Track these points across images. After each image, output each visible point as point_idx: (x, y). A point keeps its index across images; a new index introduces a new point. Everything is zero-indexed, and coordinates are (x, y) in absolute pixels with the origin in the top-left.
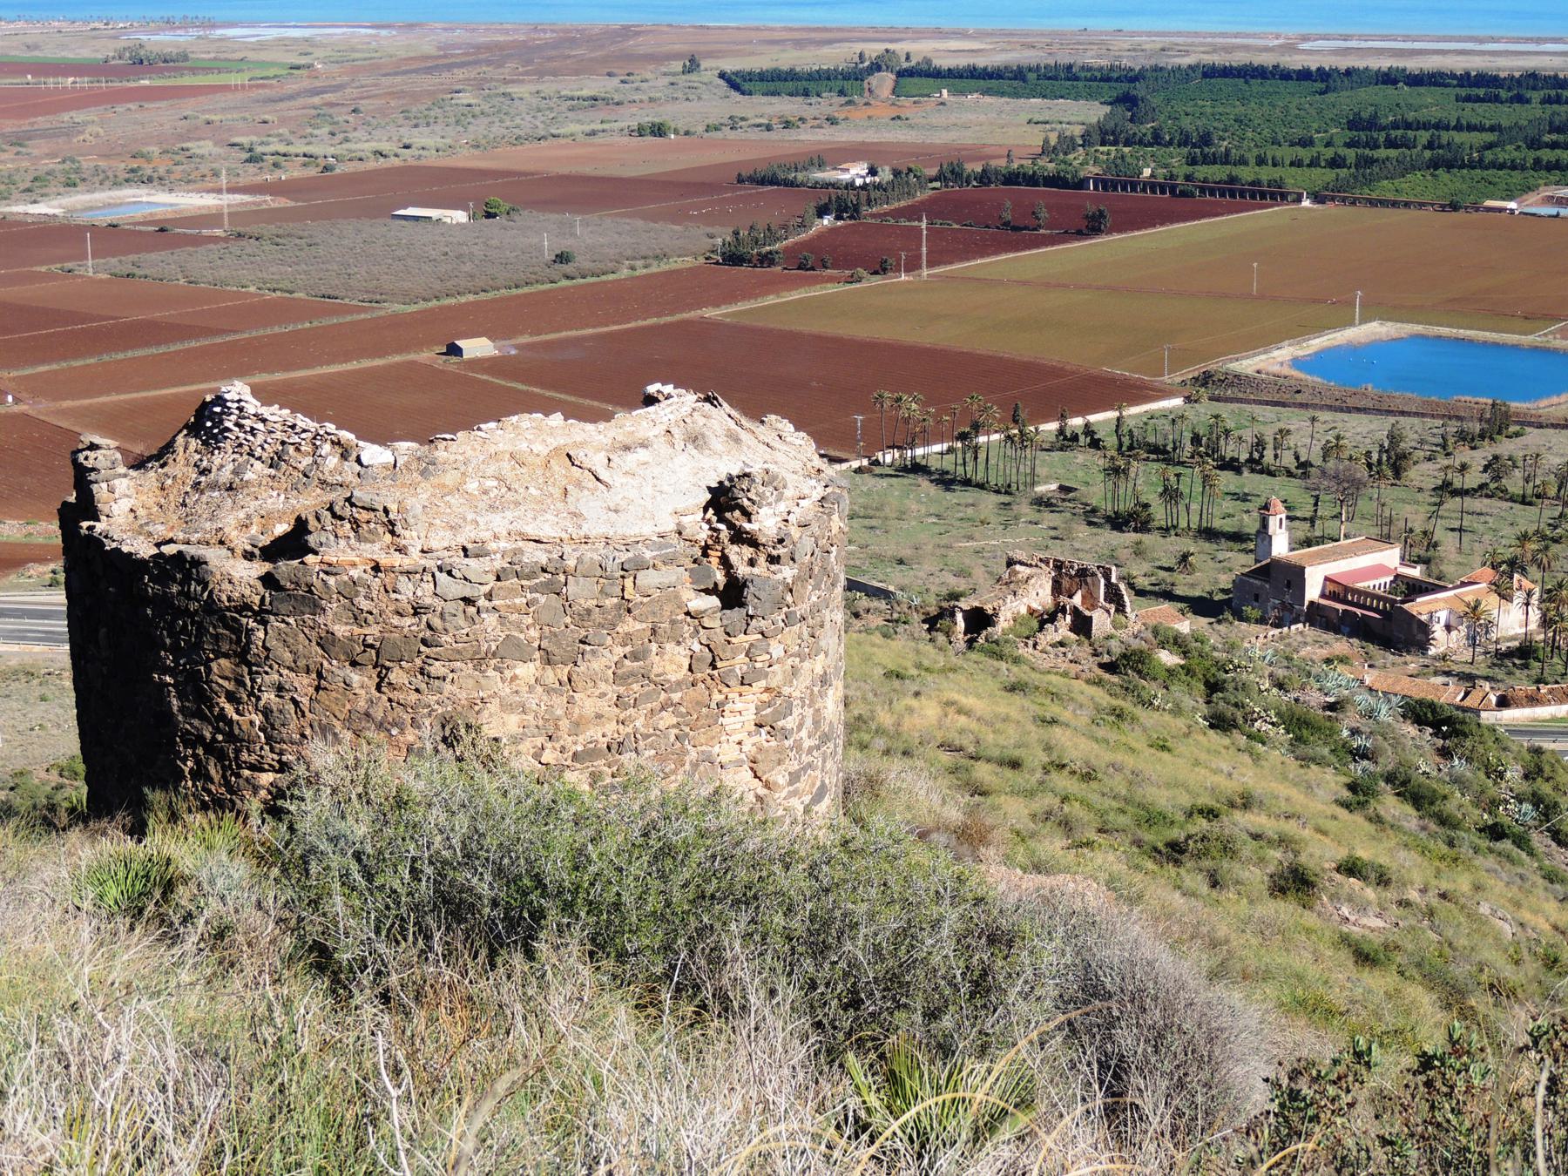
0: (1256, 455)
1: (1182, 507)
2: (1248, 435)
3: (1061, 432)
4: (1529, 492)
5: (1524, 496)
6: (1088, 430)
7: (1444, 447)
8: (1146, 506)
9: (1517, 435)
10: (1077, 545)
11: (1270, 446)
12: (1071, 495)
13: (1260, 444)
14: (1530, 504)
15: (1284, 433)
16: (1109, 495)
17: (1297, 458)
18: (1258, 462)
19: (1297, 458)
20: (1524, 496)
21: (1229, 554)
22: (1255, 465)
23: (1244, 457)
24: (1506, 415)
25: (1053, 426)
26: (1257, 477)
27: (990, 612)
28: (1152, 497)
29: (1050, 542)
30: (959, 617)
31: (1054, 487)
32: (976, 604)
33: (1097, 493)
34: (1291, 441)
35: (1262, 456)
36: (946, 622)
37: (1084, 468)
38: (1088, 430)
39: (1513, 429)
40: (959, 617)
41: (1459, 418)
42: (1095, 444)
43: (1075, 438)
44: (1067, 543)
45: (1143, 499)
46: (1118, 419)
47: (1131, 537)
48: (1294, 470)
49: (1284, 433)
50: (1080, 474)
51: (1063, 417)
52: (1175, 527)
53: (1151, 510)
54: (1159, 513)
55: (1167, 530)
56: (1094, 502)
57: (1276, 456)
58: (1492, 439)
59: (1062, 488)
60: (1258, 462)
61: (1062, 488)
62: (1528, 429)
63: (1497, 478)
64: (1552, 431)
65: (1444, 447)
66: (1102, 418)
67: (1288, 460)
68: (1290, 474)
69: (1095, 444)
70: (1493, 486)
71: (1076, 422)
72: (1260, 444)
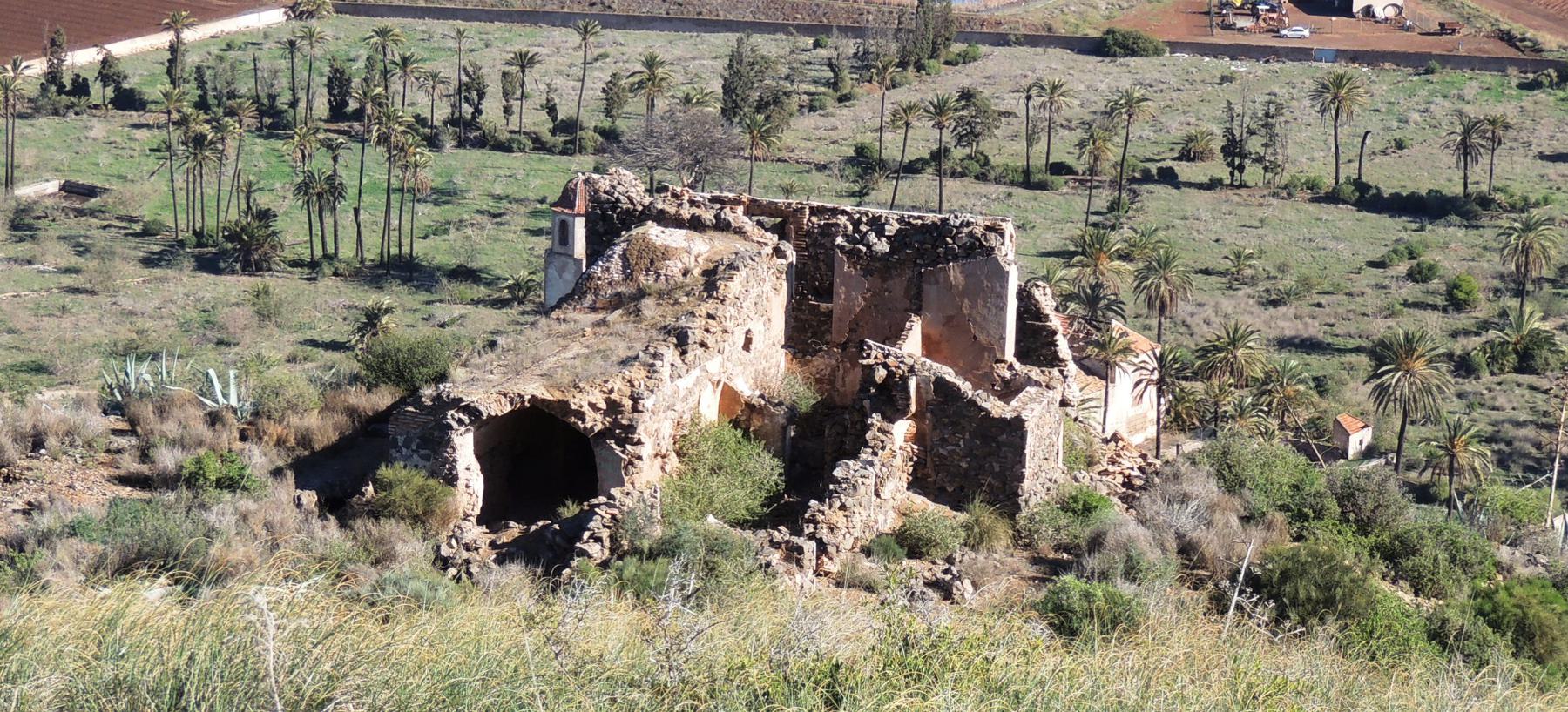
0: (467, 110)
1: (346, 220)
2: (448, 70)
3: (53, 77)
4: (1038, 160)
5: (1027, 172)
6: (108, 72)
7: (834, 85)
8: (265, 216)
9: (966, 58)
10: (127, 303)
11: (494, 87)
12: (93, 202)
13: (472, 88)
14: (1042, 186)
15: (525, 61)
16: (181, 197)
17: (551, 110)
18: (471, 124)
19: (551, 110)
20: (1027, 172)
21: (458, 310)
22: (470, 133)
23: (443, 112)
24: (947, 19)
25: (37, 67)
26: (476, 154)
27: (595, 421)
28: (279, 198)
29: (68, 299)
30: (464, 446)
31: (53, 186)
32: (533, 388)
33: (152, 193)
34: (535, 82)
35: (478, 111)
36: (404, 477)
37: (99, 144)
38: (108, 72)
39: (957, 48)
40: (464, 446)
41: (858, 31)
42: (127, 100)
43: (81, 88)
44: (104, 299)
45: (263, 200)
46: (173, 49)
47: (236, 285)
48: (546, 136)
49: (525, 61)
50: (104, 159)
51: (54, 48)
52: (329, 258)
53: (277, 225)
54: (293, 230)
55: (314, 265)
56: (146, 212)
57: (507, 111)
58: (920, 67)
59: (69, 189)
60: (471, 124)
61: (69, 189)
62: (984, 49)
63: (968, 135)
64: (1026, 49)
65: (834, 85)
66: (137, 50)
67: (535, 120)
68: (540, 145)
69: (127, 100)
70: (958, 153)
71: (82, 59)
72: (472, 88)
